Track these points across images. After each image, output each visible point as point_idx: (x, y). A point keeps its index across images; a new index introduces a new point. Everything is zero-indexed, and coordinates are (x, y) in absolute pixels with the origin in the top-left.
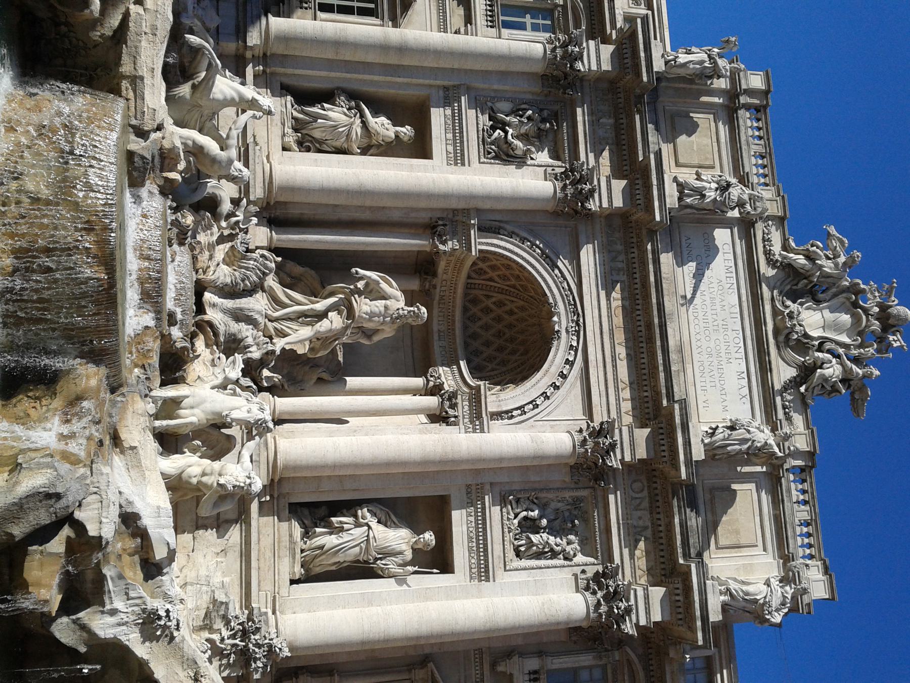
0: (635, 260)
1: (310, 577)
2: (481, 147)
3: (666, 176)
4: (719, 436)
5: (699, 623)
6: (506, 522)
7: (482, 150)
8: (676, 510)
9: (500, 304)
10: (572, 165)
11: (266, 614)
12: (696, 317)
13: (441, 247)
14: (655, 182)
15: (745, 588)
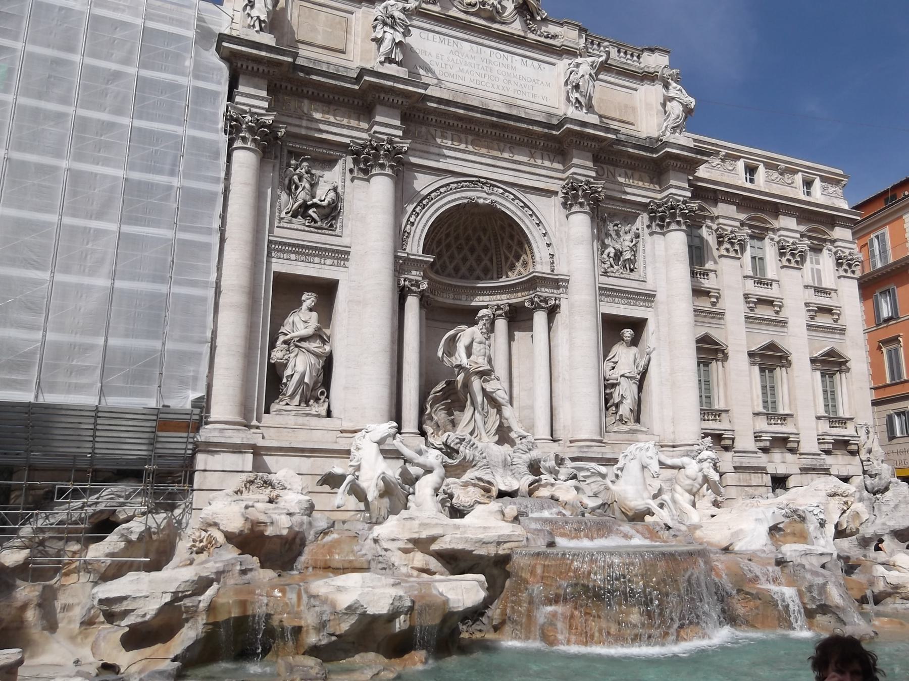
0: (439, 119)
1: (638, 420)
2: (327, 232)
3: (380, 70)
4: (581, 99)
5: (699, 157)
6: (617, 275)
7: (330, 232)
8: (625, 149)
9: (439, 243)
10: (353, 153)
11: (688, 451)
12: (481, 83)
13: (424, 286)
14: (390, 83)
15: (673, 116)
